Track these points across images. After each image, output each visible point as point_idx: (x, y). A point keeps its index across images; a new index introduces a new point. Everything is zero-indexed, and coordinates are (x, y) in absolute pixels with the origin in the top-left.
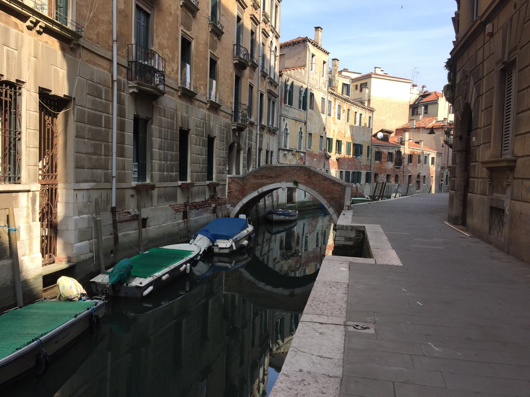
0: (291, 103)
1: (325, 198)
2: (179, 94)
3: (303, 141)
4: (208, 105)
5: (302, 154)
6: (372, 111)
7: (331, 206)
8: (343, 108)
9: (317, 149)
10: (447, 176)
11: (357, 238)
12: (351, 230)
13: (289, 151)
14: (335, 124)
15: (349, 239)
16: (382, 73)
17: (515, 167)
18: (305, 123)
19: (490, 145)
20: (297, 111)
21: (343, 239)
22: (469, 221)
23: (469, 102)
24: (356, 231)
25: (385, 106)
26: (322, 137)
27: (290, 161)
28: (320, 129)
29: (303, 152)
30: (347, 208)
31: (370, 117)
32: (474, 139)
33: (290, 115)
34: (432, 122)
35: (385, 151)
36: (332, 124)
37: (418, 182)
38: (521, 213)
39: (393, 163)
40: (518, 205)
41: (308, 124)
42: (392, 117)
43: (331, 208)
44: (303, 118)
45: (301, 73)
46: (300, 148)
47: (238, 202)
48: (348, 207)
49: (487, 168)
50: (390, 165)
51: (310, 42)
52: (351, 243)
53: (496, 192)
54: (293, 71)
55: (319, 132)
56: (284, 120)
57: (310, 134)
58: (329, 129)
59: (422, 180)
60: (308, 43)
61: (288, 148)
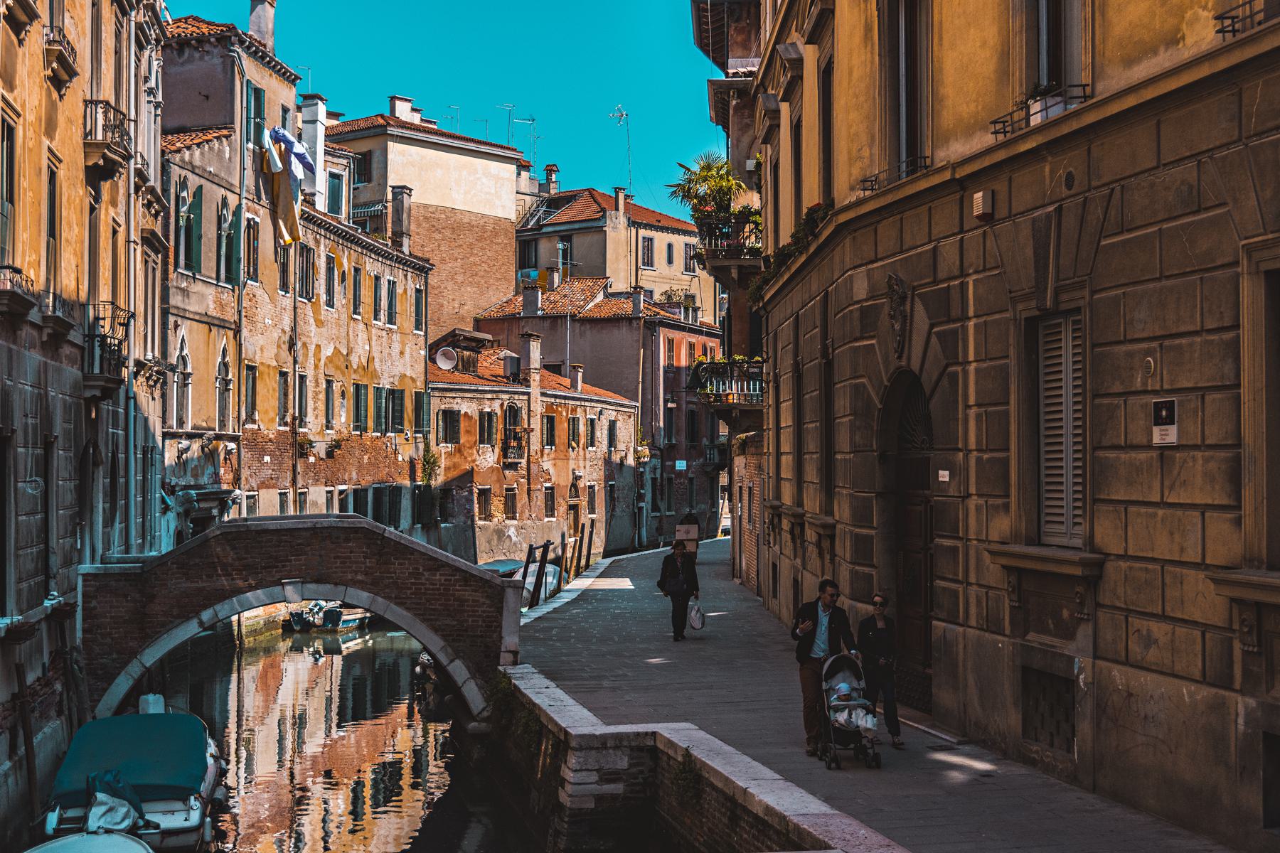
0: (193, 264)
1: (436, 630)
2: (45, 338)
3: (232, 398)
4: (48, 331)
5: (232, 446)
6: (422, 268)
7: (457, 654)
8: (342, 265)
9: (272, 420)
10: (654, 480)
11: (634, 770)
12: (616, 748)
13: (190, 436)
14: (319, 323)
15: (608, 776)
16: (416, 119)
17: (1100, 577)
18: (237, 332)
19: (1006, 507)
20: (210, 292)
21: (594, 777)
22: (945, 697)
23: (915, 365)
24: (632, 748)
25: (438, 236)
26: (283, 375)
27: (195, 476)
28: (279, 346)
29: (235, 439)
30: (510, 657)
31: (418, 291)
32: (944, 476)
33: (193, 306)
34: (594, 296)
35: (466, 407)
36: (313, 328)
37: (574, 508)
38: (1130, 695)
39: (497, 450)
40: (1119, 675)
41: (245, 332)
42: (460, 278)
43: (458, 663)
44: (231, 316)
45: (221, 152)
46: (223, 424)
47: (124, 664)
48: (515, 653)
49: (1004, 567)
50: (488, 458)
51: (242, 42)
52: (617, 788)
53: (1038, 632)
54: (197, 153)
55: (277, 357)
56: (176, 326)
57: (251, 369)
58: (304, 345)
59: (584, 502)
60: (237, 48)
61: (188, 428)
